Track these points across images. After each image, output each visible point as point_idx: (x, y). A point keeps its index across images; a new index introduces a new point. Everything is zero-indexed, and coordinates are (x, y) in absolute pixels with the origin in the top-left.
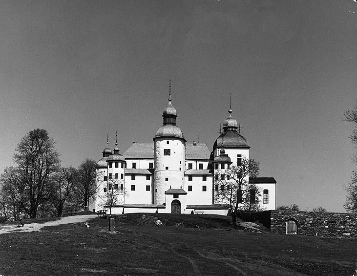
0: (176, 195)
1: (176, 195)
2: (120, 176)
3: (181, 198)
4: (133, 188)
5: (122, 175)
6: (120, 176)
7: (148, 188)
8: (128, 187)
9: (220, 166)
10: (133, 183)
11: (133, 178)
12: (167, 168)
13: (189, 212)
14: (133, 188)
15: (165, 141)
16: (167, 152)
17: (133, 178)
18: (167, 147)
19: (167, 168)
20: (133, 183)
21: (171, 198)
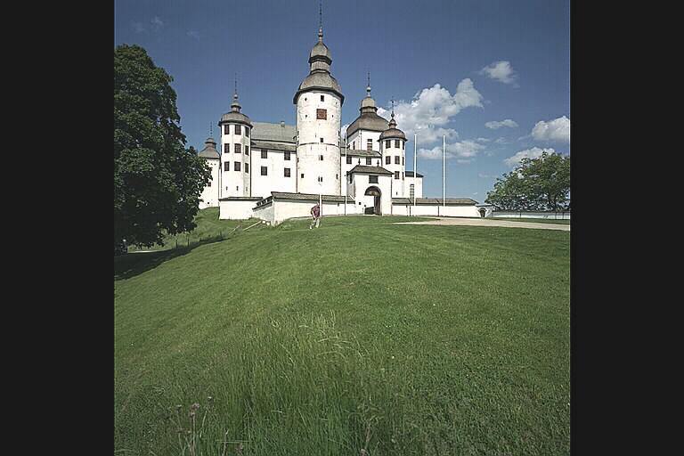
0: (373, 179)
1: (373, 179)
2: (243, 150)
3: (383, 183)
4: (264, 171)
5: (247, 147)
6: (243, 150)
7: (287, 173)
8: (256, 170)
9: (393, 142)
10: (264, 162)
11: (264, 156)
12: (322, 140)
13: (401, 211)
14: (264, 171)
15: (318, 95)
16: (321, 114)
17: (264, 156)
18: (322, 106)
19: (322, 140)
20: (264, 162)
21: (362, 182)
